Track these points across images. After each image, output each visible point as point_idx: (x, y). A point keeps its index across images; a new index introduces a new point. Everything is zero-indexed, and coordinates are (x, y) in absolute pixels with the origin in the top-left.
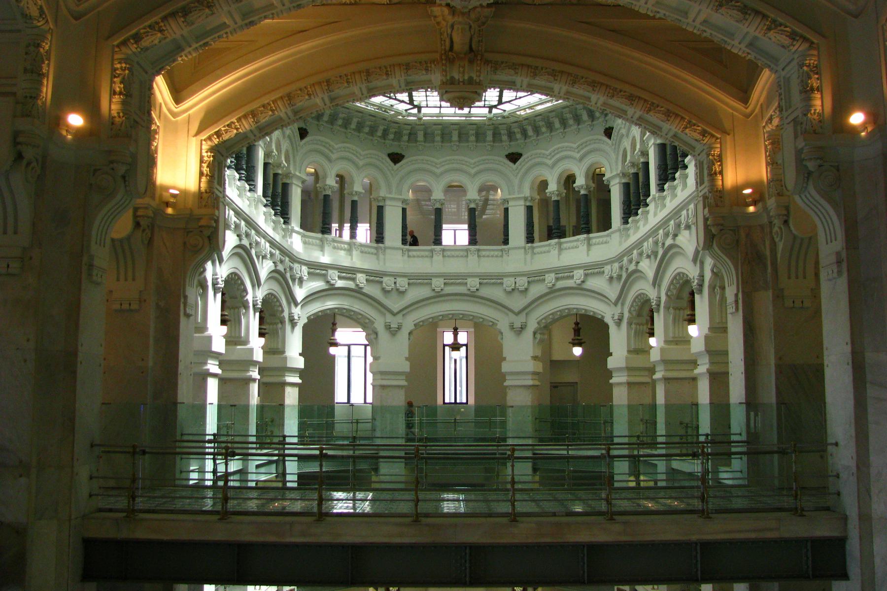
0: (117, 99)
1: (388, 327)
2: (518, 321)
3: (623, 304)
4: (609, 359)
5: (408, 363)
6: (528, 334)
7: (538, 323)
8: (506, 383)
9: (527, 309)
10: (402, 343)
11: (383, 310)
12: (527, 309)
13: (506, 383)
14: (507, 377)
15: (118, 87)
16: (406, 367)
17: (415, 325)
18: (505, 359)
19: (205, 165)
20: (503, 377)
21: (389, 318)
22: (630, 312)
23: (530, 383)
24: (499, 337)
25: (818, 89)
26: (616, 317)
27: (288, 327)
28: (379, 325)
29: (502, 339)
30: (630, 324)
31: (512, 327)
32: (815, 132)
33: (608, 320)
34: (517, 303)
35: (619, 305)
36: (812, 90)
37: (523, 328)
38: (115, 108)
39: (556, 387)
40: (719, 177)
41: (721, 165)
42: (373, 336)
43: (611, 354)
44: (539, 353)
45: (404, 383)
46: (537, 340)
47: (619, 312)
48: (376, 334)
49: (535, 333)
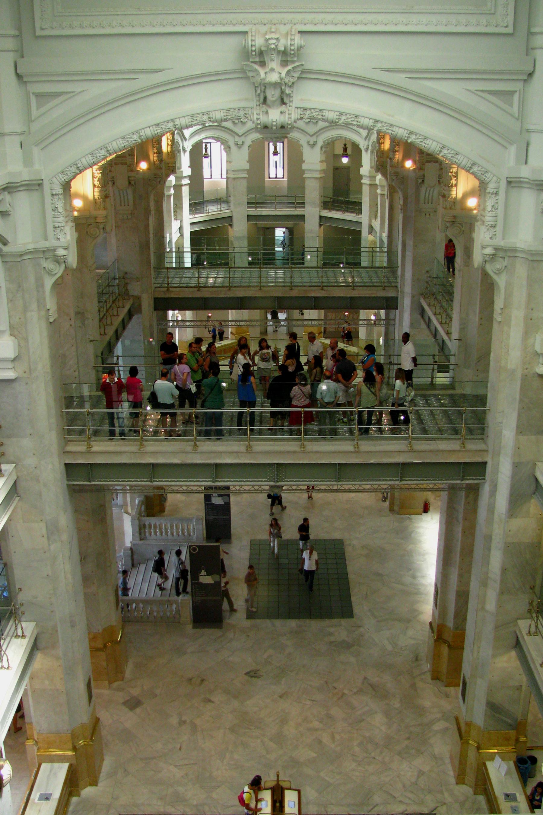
0: (155, 155)
1: (236, 144)
2: (312, 140)
3: (369, 140)
4: (361, 169)
5: (248, 164)
6: (318, 148)
7: (324, 142)
8: (304, 176)
9: (317, 133)
10: (245, 152)
11: (233, 134)
12: (317, 133)
13: (304, 176)
14: (306, 172)
15: (155, 151)
16: (247, 166)
17: (252, 142)
18: (304, 162)
19: (169, 141)
20: (303, 172)
21: (237, 139)
22: (372, 146)
23: (319, 176)
24: (301, 149)
25: (398, 151)
26: (365, 147)
27: (182, 153)
28: (231, 143)
29: (303, 150)
30: (372, 152)
31: (308, 143)
32: (395, 167)
33: (361, 146)
34: (312, 129)
35: (367, 140)
36: (396, 151)
37: (315, 144)
38: (155, 158)
39: (337, 169)
40: (382, 145)
41: (384, 140)
42: (228, 149)
43: (362, 166)
44: (324, 158)
45: (247, 176)
46: (323, 152)
47: (367, 144)
48: (230, 148)
49: (321, 147)
